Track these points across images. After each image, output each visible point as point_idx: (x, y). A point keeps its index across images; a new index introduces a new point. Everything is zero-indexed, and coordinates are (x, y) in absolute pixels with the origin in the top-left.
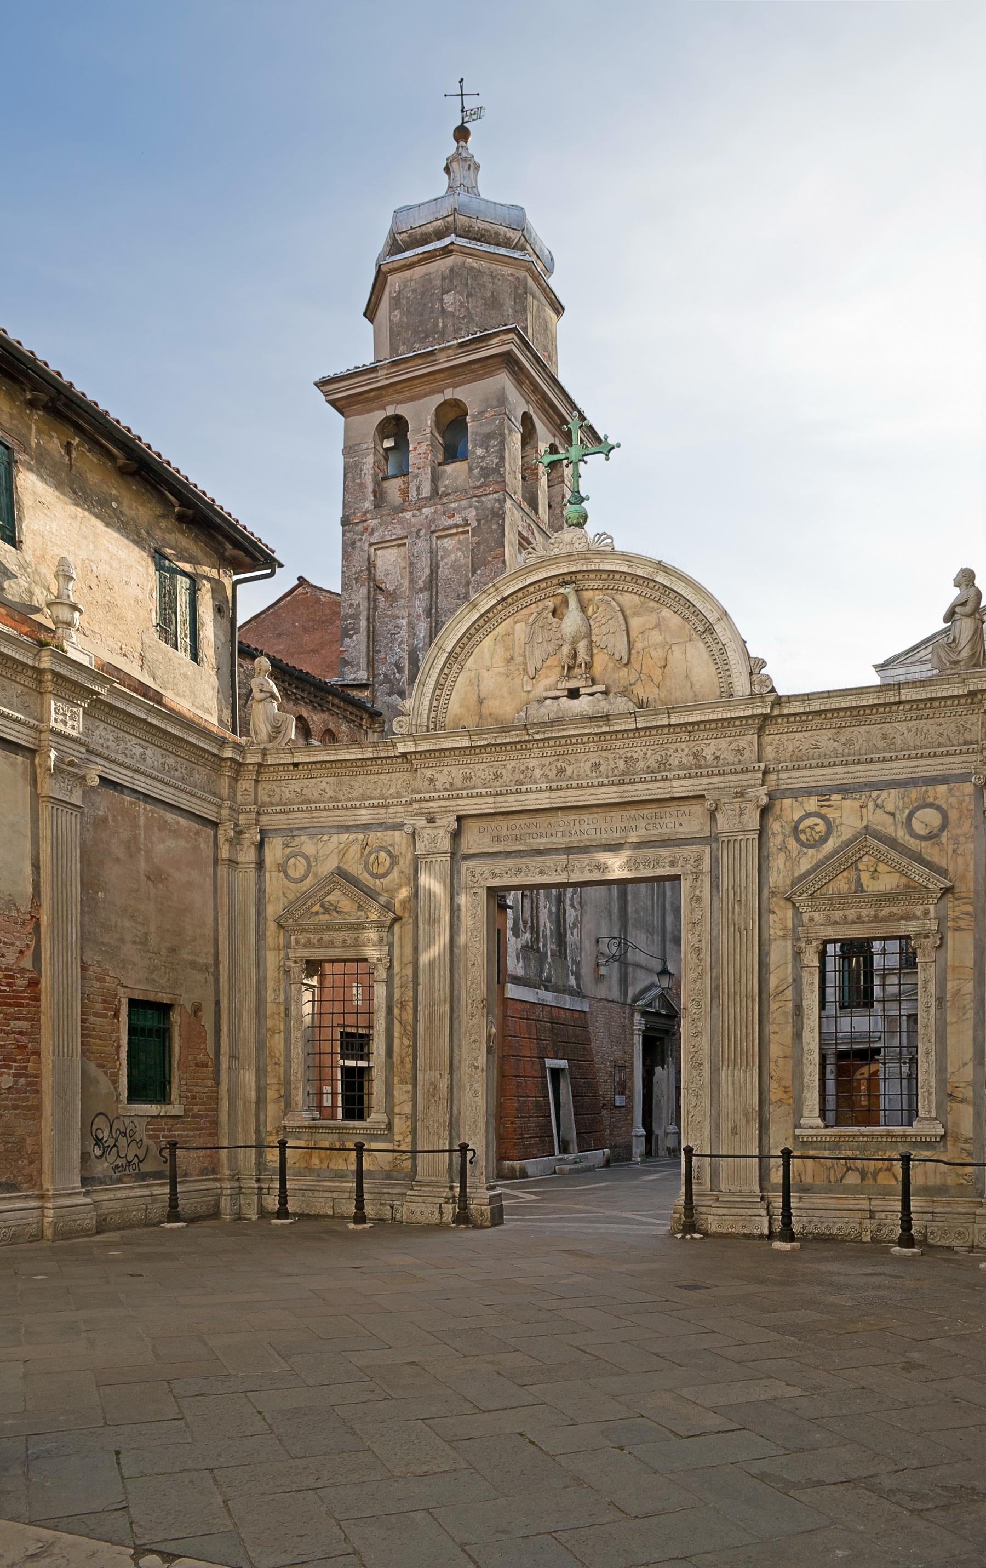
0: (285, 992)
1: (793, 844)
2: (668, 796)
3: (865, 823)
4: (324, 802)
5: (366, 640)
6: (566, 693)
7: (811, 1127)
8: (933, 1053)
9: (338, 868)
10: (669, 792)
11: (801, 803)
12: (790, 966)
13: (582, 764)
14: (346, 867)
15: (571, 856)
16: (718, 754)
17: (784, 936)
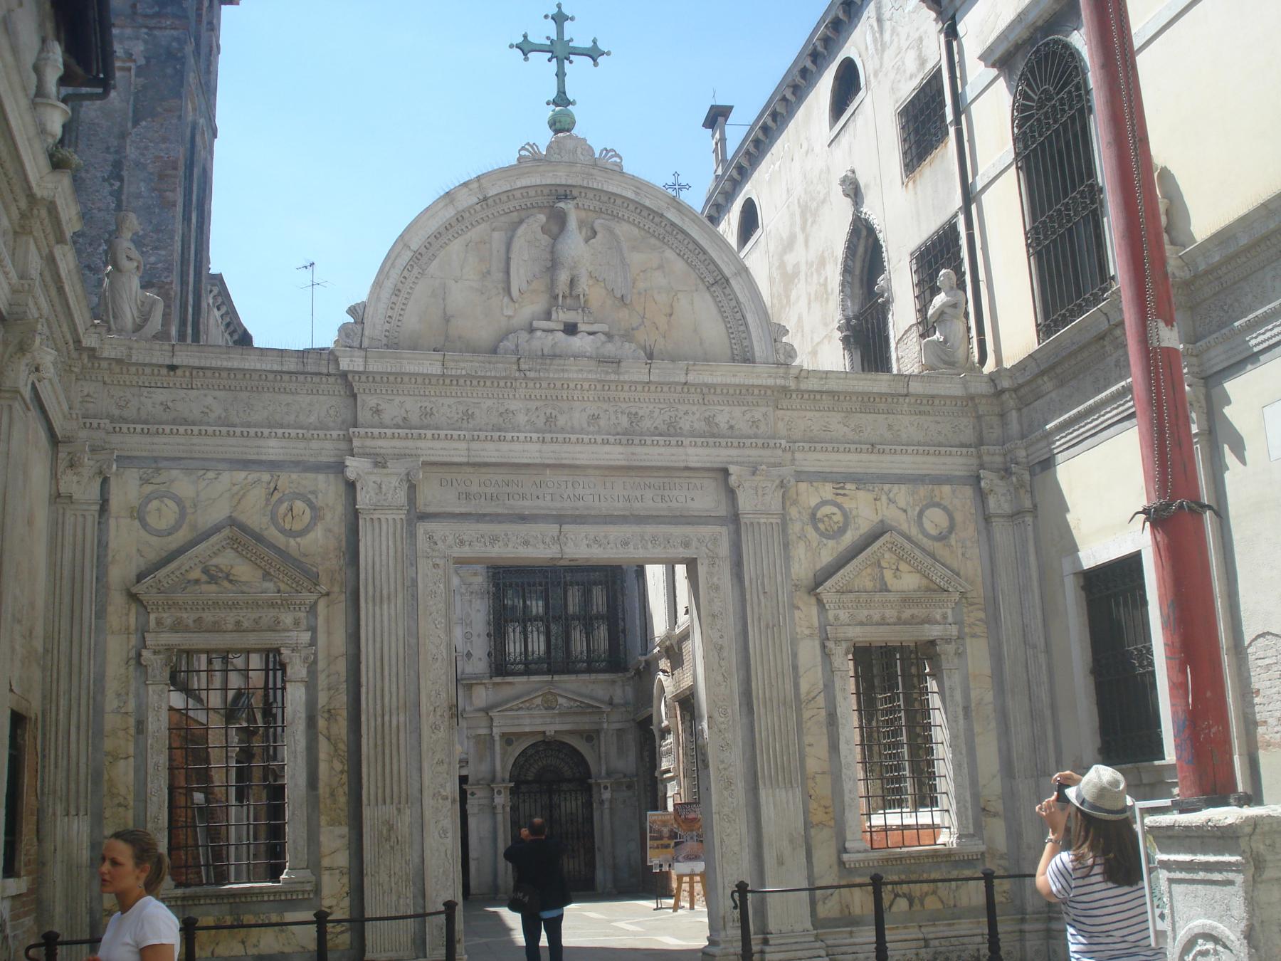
0: (138, 696)
1: (811, 534)
3: (880, 518)
4: (208, 424)
6: (562, 327)
7: (859, 852)
8: (966, 766)
11: (817, 489)
12: (820, 669)
14: (242, 518)
15: (564, 527)
16: (733, 423)
17: (811, 636)
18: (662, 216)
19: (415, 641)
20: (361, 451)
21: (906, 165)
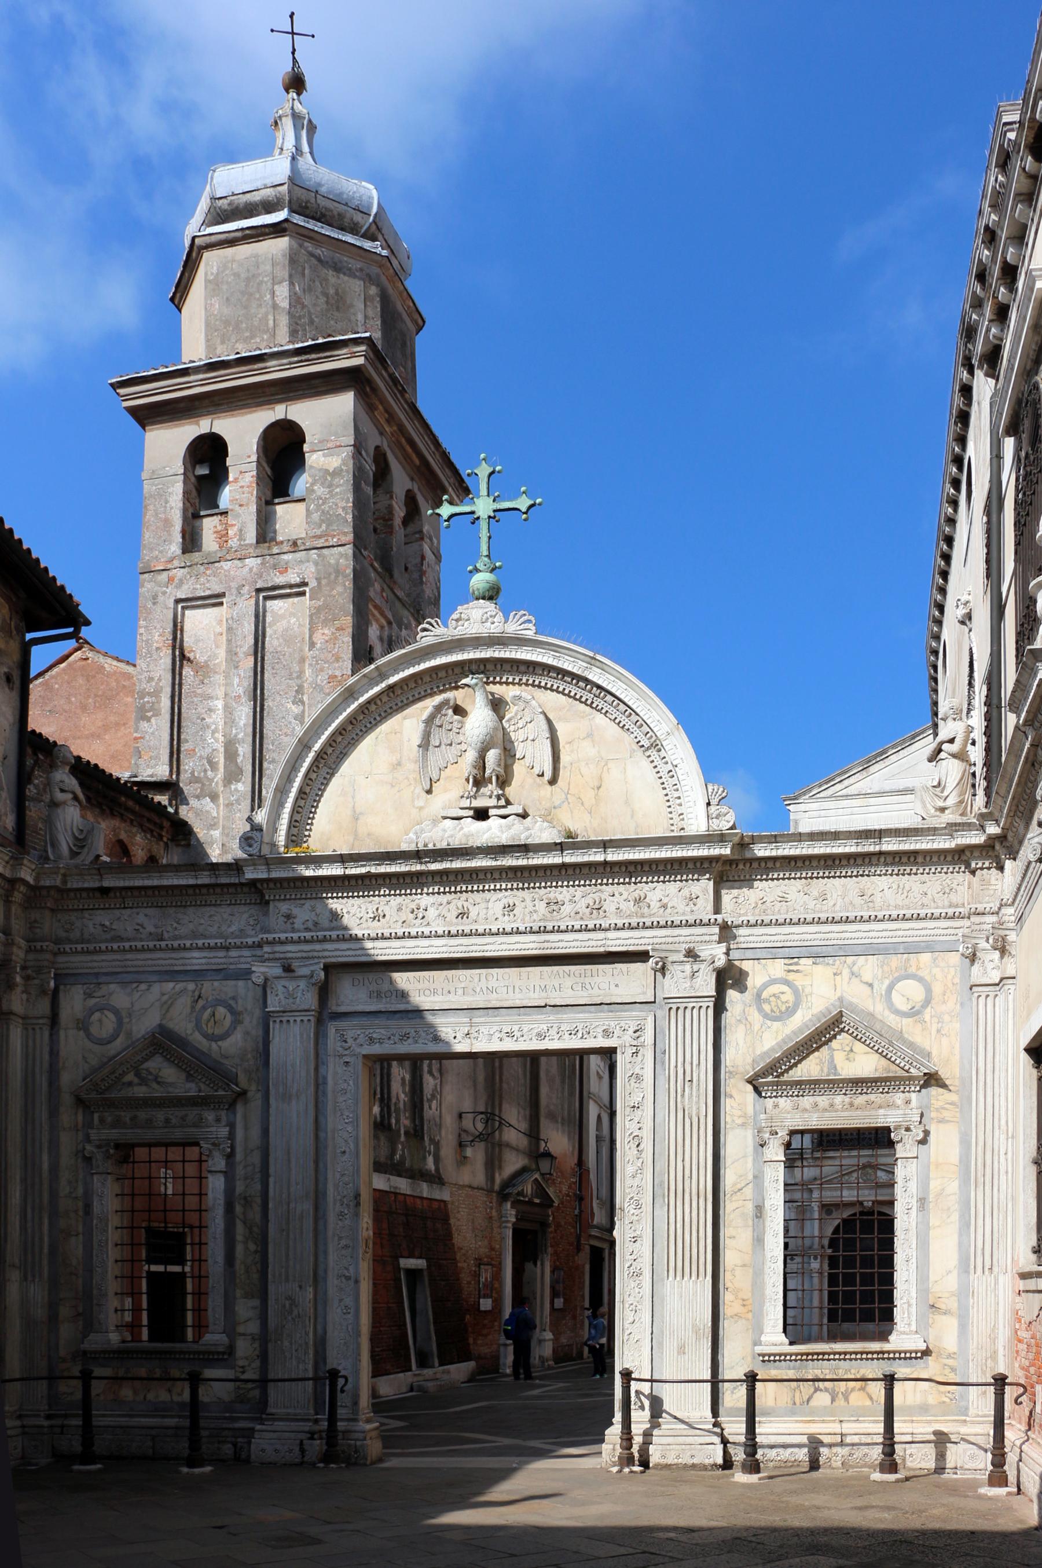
1: (755, 1017)
2: (602, 950)
5: (169, 725)
6: (471, 813)
14: (171, 1025)
16: (665, 900)
20: (271, 956)
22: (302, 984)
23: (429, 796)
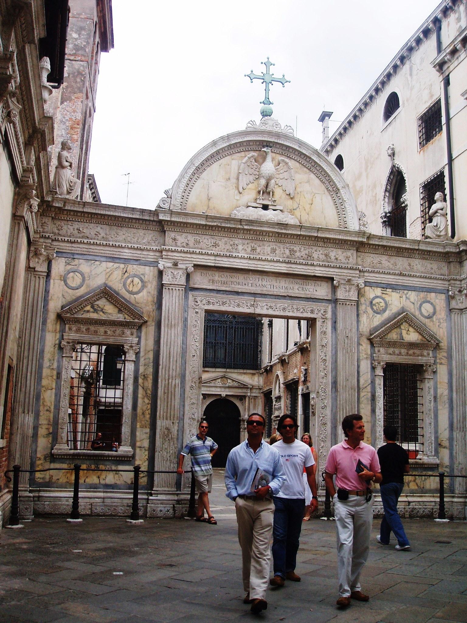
0: (58, 362)
2: (313, 274)
3: (402, 306)
6: (261, 206)
8: (433, 424)
9: (105, 283)
10: (313, 273)
11: (374, 290)
12: (369, 374)
13: (266, 247)
14: (110, 284)
15: (257, 299)
16: (337, 256)
17: (367, 358)
18: (310, 158)
19: (185, 346)
20: (166, 257)
21: (420, 143)
22: (181, 272)
23: (241, 195)
